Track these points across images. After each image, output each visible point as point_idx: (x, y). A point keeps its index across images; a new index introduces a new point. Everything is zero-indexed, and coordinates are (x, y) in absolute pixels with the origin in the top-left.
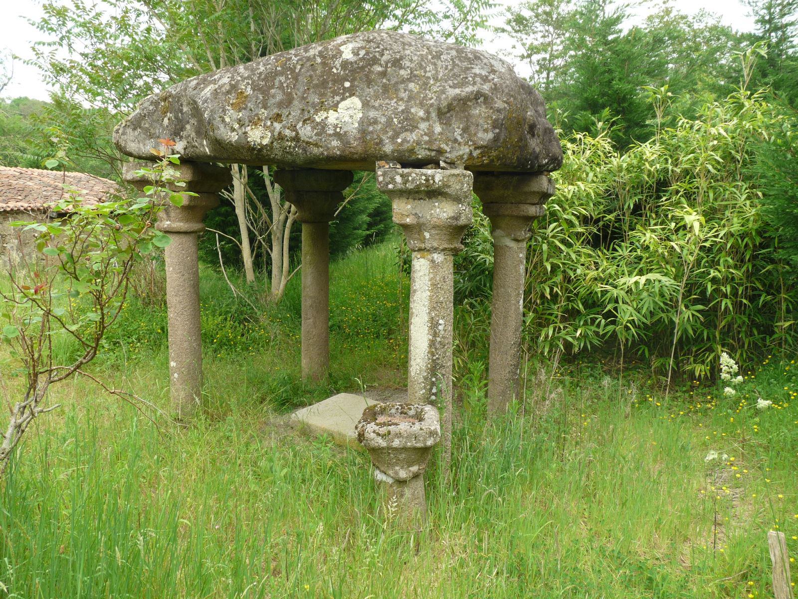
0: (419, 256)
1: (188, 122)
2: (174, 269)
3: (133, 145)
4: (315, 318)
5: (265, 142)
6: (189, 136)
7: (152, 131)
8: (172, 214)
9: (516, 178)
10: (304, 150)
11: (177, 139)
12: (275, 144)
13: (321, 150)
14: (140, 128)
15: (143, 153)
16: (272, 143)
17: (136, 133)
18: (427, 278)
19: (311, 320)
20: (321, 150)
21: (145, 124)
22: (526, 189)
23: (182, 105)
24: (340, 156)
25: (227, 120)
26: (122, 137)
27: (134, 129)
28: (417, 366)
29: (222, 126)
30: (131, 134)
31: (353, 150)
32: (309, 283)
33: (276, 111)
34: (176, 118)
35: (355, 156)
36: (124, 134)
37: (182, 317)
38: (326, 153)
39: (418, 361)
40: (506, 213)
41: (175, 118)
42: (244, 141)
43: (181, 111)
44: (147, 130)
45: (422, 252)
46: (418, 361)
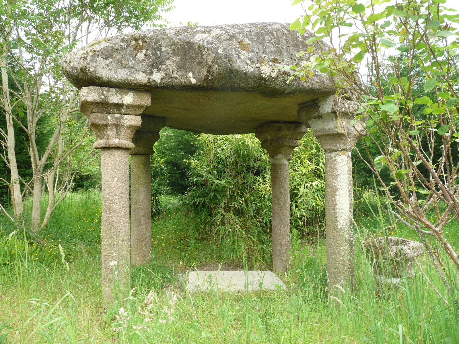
0: (341, 154)
1: (168, 59)
2: (118, 179)
3: (104, 71)
4: (147, 224)
5: (274, 75)
6: (168, 69)
7: (124, 62)
8: (122, 133)
9: (294, 125)
10: (298, 83)
11: (155, 71)
12: (280, 77)
13: (309, 84)
14: (111, 58)
15: (115, 79)
16: (278, 76)
17: (107, 62)
18: (346, 166)
19: (144, 226)
20: (309, 84)
21: (116, 56)
22: (300, 131)
23: (161, 45)
24: (318, 89)
25: (242, 57)
26: (91, 63)
27: (105, 59)
28: (344, 221)
29: (239, 61)
30: (100, 60)
31: (325, 86)
32: (142, 199)
33: (273, 56)
34: (154, 54)
35: (326, 90)
36: (93, 61)
37: (124, 219)
38: (311, 86)
39: (344, 217)
40: (287, 144)
41: (152, 54)
42: (257, 73)
43: (160, 50)
44: (119, 62)
45: (343, 151)
46: (344, 217)
